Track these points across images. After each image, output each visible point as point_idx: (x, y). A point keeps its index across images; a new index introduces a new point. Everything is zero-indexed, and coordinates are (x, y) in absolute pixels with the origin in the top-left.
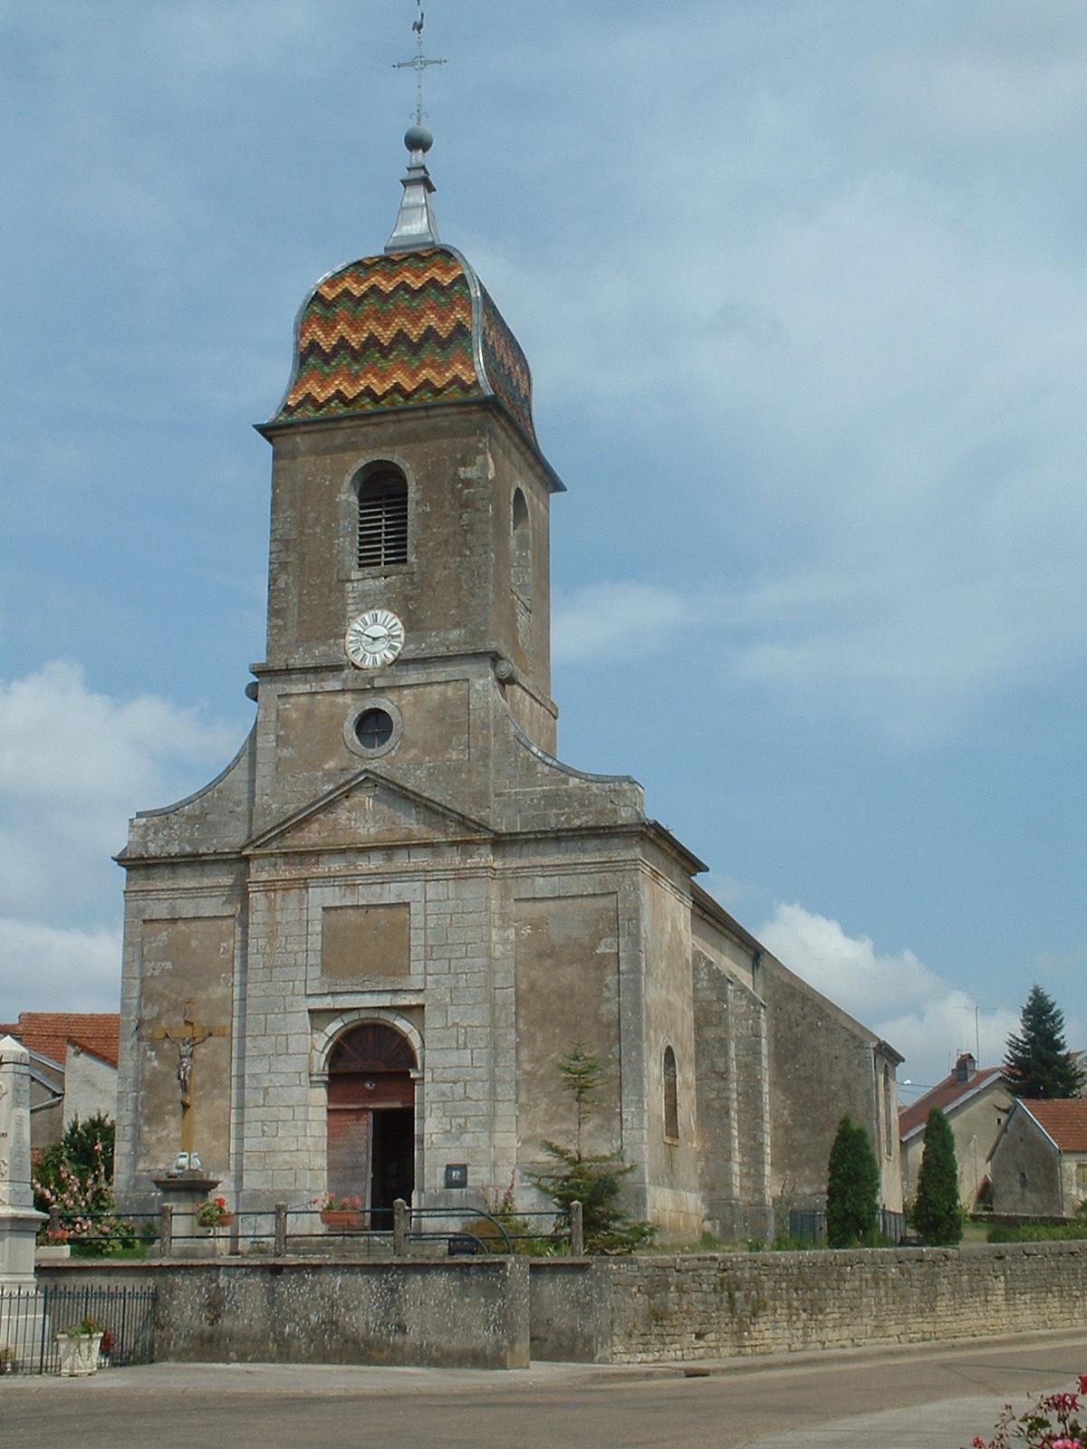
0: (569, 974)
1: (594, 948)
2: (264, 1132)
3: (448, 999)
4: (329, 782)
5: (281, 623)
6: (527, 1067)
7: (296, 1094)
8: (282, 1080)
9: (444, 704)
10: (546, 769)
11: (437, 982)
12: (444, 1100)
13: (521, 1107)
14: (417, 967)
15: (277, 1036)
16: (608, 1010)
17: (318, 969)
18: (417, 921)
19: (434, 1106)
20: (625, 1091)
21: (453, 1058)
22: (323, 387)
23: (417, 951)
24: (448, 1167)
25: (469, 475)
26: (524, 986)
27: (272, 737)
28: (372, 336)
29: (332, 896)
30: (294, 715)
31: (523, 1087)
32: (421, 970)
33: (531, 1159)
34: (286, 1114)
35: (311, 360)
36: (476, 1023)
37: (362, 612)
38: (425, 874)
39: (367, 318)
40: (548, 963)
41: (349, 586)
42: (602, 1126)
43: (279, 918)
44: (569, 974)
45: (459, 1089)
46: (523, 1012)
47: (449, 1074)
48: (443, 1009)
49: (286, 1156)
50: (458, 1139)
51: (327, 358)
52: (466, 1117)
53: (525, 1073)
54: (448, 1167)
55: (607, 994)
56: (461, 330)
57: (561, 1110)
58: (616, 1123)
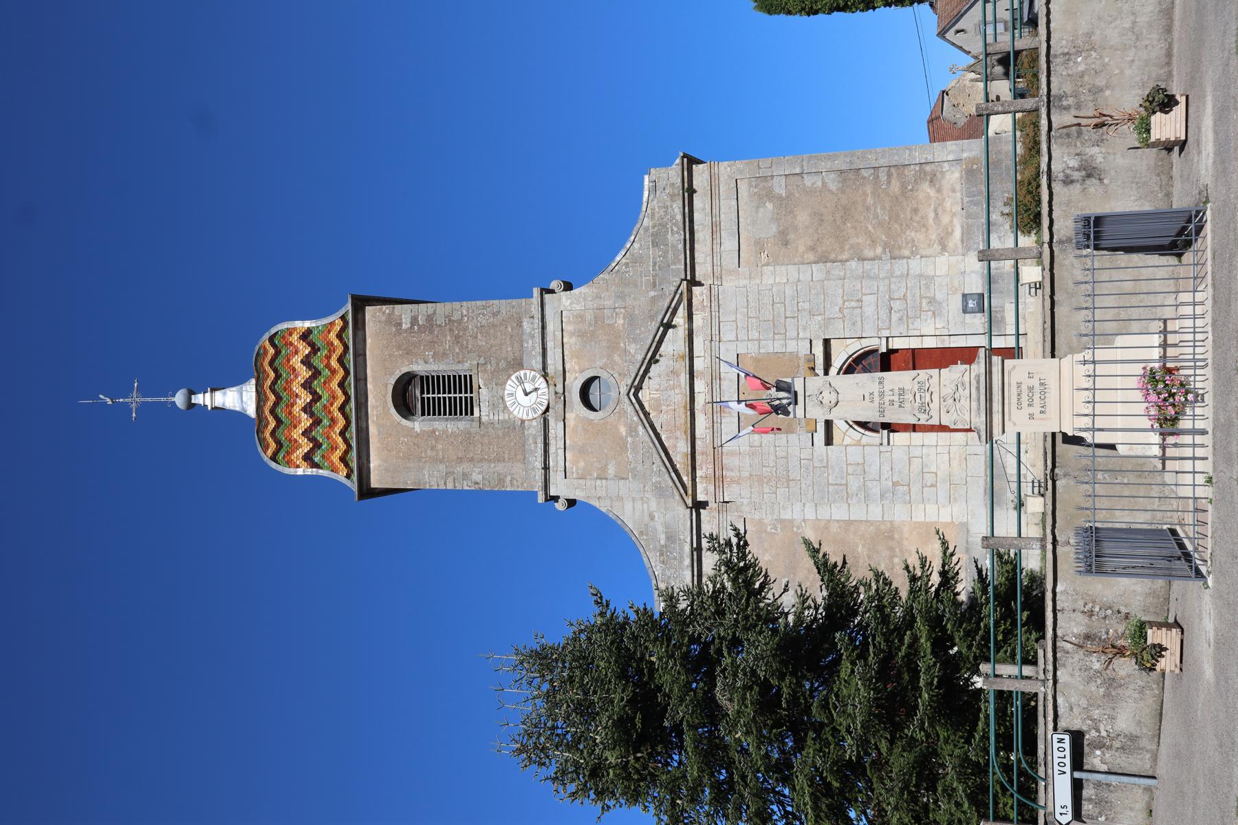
0: (803, 217)
1: (780, 198)
2: (932, 486)
3: (819, 318)
4: (636, 431)
5: (509, 478)
6: (879, 250)
7: (899, 454)
8: (886, 468)
9: (581, 334)
10: (636, 245)
11: (805, 329)
12: (906, 319)
13: (914, 253)
14: (792, 346)
15: (848, 474)
16: (833, 183)
17: (791, 436)
18: (752, 349)
19: (911, 326)
20: (902, 161)
21: (869, 310)
23: (778, 347)
24: (965, 311)
25: (409, 320)
26: (811, 256)
27: (598, 482)
28: (304, 410)
29: (729, 426)
30: (582, 464)
31: (897, 252)
32: (794, 343)
33: (959, 243)
34: (916, 463)
35: (317, 459)
36: (840, 291)
37: (505, 407)
38: (715, 339)
39: (290, 413)
40: (791, 236)
41: (484, 419)
42: (931, 181)
43: (747, 474)
44: (803, 217)
45: (896, 305)
46: (833, 256)
47: (883, 314)
48: (828, 322)
49: (955, 463)
50: (940, 303)
51: (317, 445)
52: (921, 298)
53: (884, 252)
54: (965, 311)
55: (819, 184)
56: (306, 336)
57: (917, 218)
58: (928, 168)
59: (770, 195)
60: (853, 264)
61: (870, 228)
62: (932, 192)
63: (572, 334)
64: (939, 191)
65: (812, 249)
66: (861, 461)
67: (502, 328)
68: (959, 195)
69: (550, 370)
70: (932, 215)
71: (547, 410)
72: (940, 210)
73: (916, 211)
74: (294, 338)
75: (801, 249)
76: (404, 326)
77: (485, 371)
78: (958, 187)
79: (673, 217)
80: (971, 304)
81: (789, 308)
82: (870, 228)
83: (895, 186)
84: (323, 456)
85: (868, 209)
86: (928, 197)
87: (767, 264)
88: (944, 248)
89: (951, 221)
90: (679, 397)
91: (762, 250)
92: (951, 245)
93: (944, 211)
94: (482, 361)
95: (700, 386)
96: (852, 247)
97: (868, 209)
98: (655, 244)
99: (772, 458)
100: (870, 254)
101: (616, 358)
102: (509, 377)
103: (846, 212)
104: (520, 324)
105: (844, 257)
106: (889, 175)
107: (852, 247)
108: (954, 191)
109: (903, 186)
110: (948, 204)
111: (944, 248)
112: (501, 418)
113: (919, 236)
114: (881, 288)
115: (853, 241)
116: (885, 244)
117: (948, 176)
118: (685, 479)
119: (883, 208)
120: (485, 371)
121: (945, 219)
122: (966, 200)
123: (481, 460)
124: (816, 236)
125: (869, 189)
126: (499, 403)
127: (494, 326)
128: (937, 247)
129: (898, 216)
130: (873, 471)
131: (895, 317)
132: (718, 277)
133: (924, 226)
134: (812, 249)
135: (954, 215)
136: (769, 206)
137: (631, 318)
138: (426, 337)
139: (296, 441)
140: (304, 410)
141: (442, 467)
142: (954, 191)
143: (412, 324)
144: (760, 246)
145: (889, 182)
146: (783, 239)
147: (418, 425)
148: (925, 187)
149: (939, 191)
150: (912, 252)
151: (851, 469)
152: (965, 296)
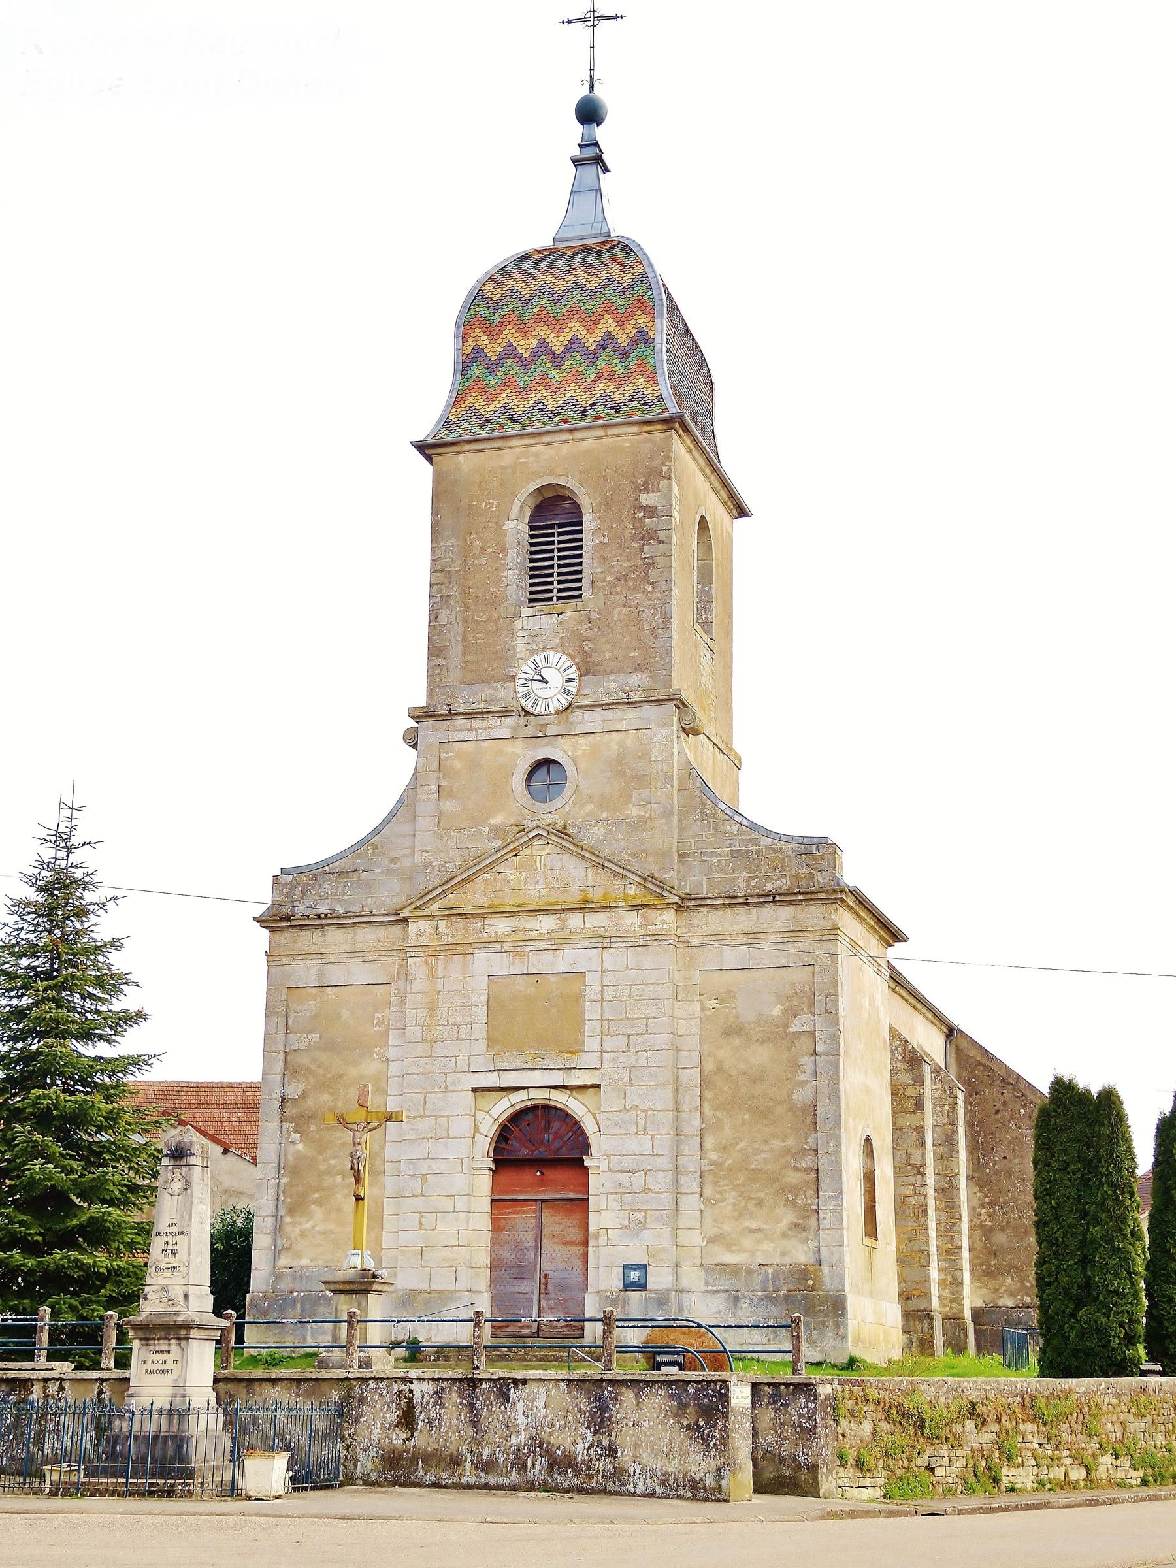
0: (760, 1055)
1: (787, 1026)
2: (421, 1224)
3: (626, 1079)
4: (496, 838)
5: (442, 662)
6: (713, 1156)
7: (459, 1183)
8: (443, 1166)
9: (621, 758)
10: (736, 828)
11: (614, 1060)
12: (621, 1192)
13: (707, 1201)
14: (592, 1044)
15: (437, 1117)
16: (802, 1095)
17: (483, 1044)
18: (592, 992)
19: (611, 1197)
20: (822, 1186)
21: (633, 1144)
22: (488, 400)
23: (593, 1025)
24: (626, 1267)
25: (651, 503)
26: (709, 1066)
27: (434, 789)
28: (542, 343)
29: (499, 963)
30: (458, 765)
31: (709, 1178)
32: (597, 1046)
33: (717, 1260)
34: (448, 1204)
35: (476, 370)
36: (658, 1107)
37: (532, 653)
38: (604, 940)
39: (537, 321)
40: (737, 1041)
41: (518, 623)
42: (796, 1225)
43: (440, 987)
44: (760, 1055)
45: (638, 1179)
46: (708, 1095)
47: (628, 1163)
48: (621, 1089)
49: (446, 1253)
50: (638, 1235)
51: (492, 368)
52: (646, 1210)
53: (713, 1163)
54: (626, 1267)
55: (802, 1078)
56: (643, 338)
57: (751, 1205)
58: (813, 1222)
59: (792, 1013)
60: (696, 1122)
61: (742, 1144)
62: (783, 1225)
63: (622, 745)
64: (784, 1235)
65: (720, 1069)
66: (452, 1135)
67: (635, 644)
68: (777, 1260)
69: (576, 716)
70: (754, 1225)
71: (527, 713)
72: (759, 1236)
73: (760, 1204)
74: (641, 319)
75: (721, 1054)
76: (643, 496)
77: (580, 623)
78: (787, 1260)
79: (769, 879)
80: (634, 1275)
81: (640, 1039)
82: (742, 1144)
83: (793, 1178)
84: (478, 379)
85: (766, 1142)
86: (777, 1221)
87: (703, 1009)
88: (712, 1240)
89: (745, 1251)
90: (536, 893)
91: (722, 1001)
92: (715, 1248)
93: (758, 1242)
94: (594, 616)
95: (549, 922)
96: (719, 1120)
97: (766, 1142)
98: (735, 855)
99: (459, 1020)
100: (709, 1143)
101: (590, 807)
102: (571, 657)
103: (762, 1113)
104: (638, 669)
105: (707, 1110)
106: (806, 1170)
107: (719, 1120)
108: (783, 1254)
109: (791, 1189)
110: (767, 1246)
111: (712, 1240)
112: (519, 648)
113: (727, 1208)
114: (659, 1160)
115: (727, 1122)
116: (721, 1164)
117: (802, 1248)
118: (436, 906)
119: (765, 1161)
120: (580, 623)
121: (748, 1242)
122: (770, 1270)
123: (465, 621)
124: (734, 1073)
125: (791, 1142)
126: (538, 642)
127: (640, 629)
128: (712, 1231)
129: (754, 1180)
130: (439, 1149)
131: (623, 1177)
132: (680, 943)
133: (741, 1215)
134: (720, 1069)
135: (753, 1254)
136: (777, 1011)
137: (638, 824)
138: (628, 530)
139: (500, 333)
140: (542, 343)
141: (458, 565)
142: (783, 1254)
143: (644, 509)
144: (725, 997)
145: (797, 1169)
146: (734, 1030)
147: (517, 526)
148: (788, 1217)
149: (784, 1235)
150: (708, 1200)
151: (443, 1121)
152: (644, 1267)
